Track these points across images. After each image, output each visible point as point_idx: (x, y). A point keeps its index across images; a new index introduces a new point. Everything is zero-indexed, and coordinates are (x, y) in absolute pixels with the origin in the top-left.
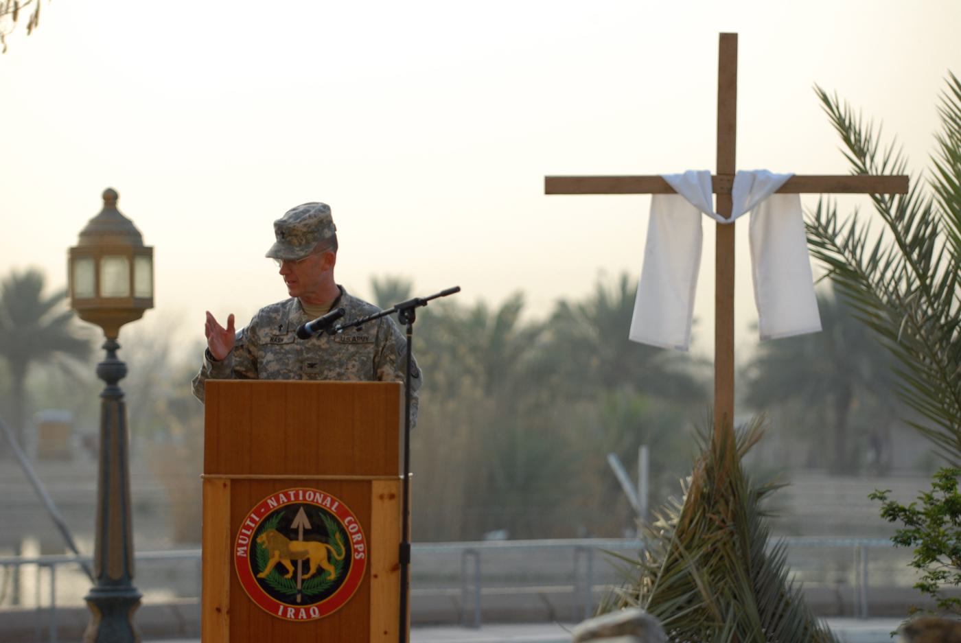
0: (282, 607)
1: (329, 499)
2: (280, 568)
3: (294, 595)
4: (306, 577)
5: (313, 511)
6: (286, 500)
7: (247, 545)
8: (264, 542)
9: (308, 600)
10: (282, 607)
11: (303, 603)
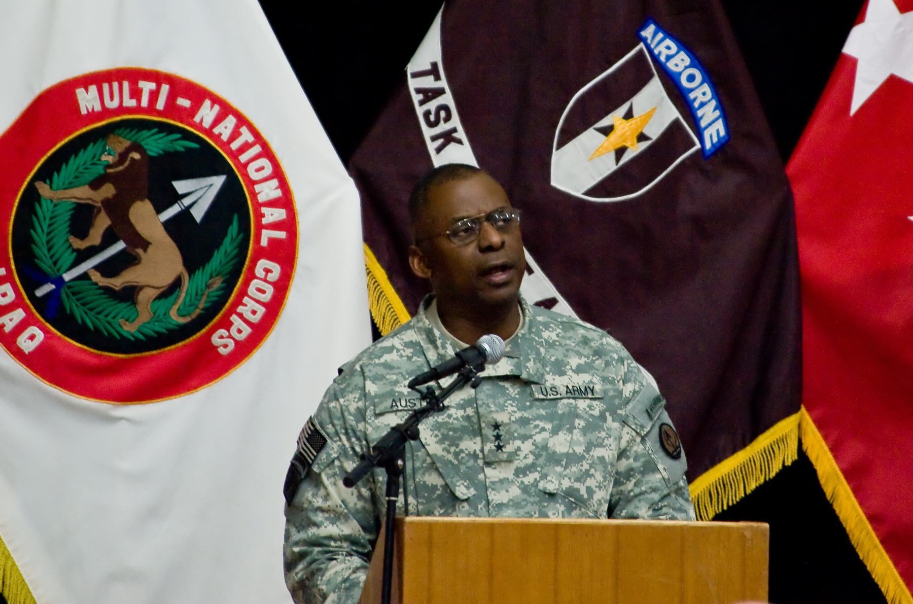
3: (44, 278)
4: (96, 277)
11: (39, 303)
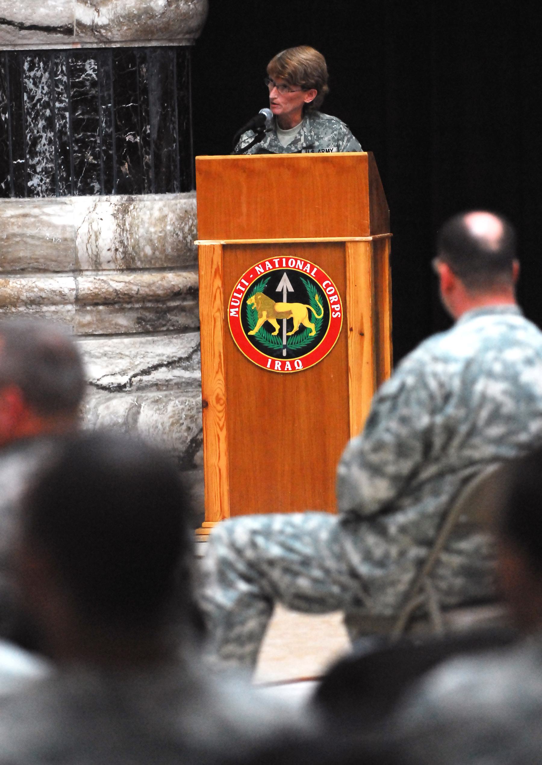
0: (270, 361)
1: (308, 265)
2: (268, 327)
3: (281, 351)
4: (290, 334)
5: (295, 277)
6: (271, 267)
7: (238, 307)
8: (253, 304)
9: (292, 354)
10: (270, 361)
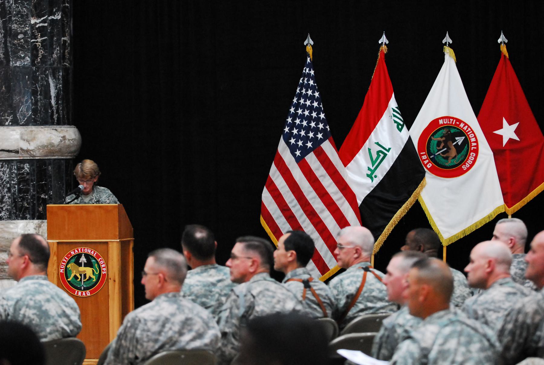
2: (76, 277)
3: (81, 287)
5: (87, 256)
